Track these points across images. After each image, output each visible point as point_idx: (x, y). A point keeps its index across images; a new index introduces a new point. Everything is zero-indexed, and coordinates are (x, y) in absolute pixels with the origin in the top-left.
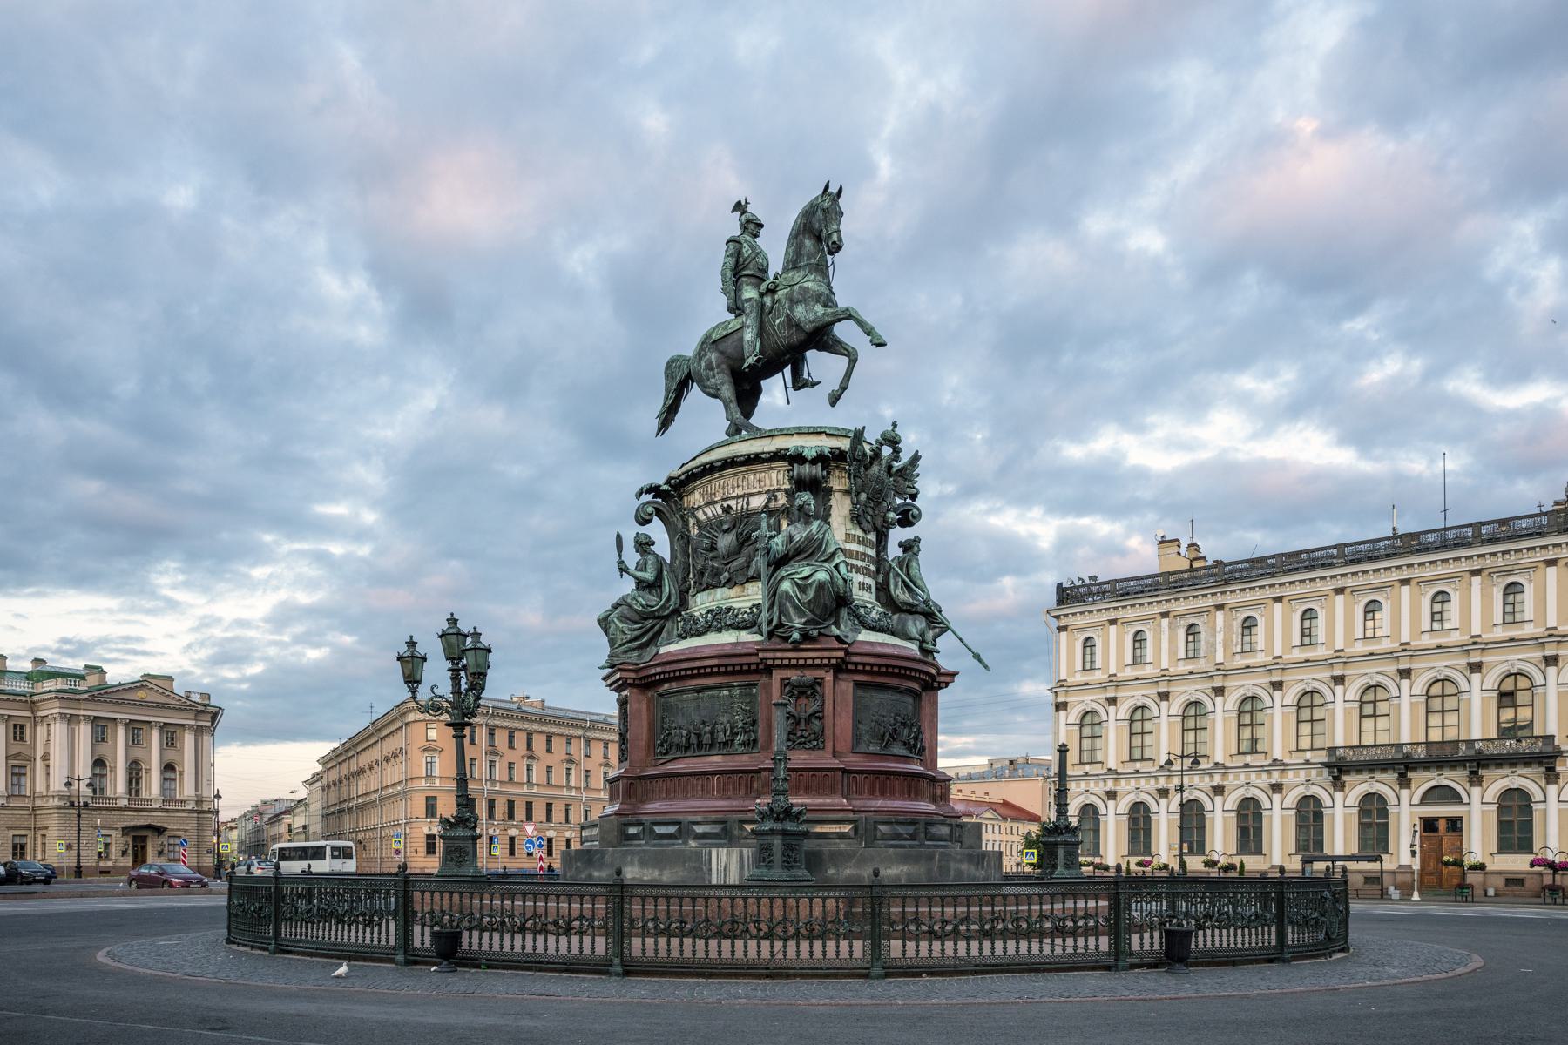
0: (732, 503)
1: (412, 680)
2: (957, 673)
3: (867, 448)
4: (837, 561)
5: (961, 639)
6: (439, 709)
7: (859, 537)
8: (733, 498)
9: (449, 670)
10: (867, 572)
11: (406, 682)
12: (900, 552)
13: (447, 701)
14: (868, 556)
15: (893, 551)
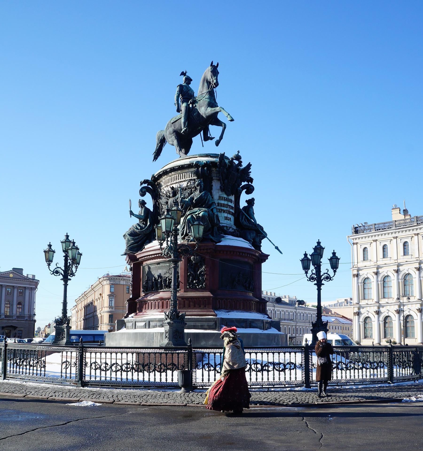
0: (174, 186)
1: (49, 261)
2: (269, 255)
3: (227, 161)
4: (212, 207)
5: (270, 241)
6: (59, 273)
7: (225, 198)
8: (174, 183)
9: (64, 256)
10: (229, 213)
11: (46, 261)
12: (246, 205)
13: (62, 270)
14: (229, 206)
15: (243, 204)
